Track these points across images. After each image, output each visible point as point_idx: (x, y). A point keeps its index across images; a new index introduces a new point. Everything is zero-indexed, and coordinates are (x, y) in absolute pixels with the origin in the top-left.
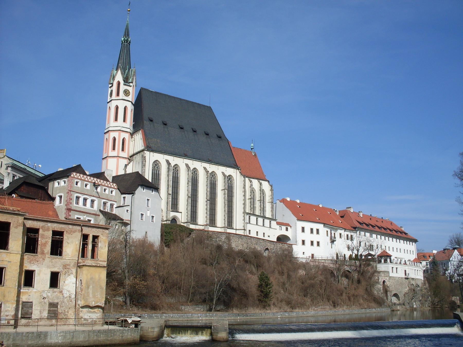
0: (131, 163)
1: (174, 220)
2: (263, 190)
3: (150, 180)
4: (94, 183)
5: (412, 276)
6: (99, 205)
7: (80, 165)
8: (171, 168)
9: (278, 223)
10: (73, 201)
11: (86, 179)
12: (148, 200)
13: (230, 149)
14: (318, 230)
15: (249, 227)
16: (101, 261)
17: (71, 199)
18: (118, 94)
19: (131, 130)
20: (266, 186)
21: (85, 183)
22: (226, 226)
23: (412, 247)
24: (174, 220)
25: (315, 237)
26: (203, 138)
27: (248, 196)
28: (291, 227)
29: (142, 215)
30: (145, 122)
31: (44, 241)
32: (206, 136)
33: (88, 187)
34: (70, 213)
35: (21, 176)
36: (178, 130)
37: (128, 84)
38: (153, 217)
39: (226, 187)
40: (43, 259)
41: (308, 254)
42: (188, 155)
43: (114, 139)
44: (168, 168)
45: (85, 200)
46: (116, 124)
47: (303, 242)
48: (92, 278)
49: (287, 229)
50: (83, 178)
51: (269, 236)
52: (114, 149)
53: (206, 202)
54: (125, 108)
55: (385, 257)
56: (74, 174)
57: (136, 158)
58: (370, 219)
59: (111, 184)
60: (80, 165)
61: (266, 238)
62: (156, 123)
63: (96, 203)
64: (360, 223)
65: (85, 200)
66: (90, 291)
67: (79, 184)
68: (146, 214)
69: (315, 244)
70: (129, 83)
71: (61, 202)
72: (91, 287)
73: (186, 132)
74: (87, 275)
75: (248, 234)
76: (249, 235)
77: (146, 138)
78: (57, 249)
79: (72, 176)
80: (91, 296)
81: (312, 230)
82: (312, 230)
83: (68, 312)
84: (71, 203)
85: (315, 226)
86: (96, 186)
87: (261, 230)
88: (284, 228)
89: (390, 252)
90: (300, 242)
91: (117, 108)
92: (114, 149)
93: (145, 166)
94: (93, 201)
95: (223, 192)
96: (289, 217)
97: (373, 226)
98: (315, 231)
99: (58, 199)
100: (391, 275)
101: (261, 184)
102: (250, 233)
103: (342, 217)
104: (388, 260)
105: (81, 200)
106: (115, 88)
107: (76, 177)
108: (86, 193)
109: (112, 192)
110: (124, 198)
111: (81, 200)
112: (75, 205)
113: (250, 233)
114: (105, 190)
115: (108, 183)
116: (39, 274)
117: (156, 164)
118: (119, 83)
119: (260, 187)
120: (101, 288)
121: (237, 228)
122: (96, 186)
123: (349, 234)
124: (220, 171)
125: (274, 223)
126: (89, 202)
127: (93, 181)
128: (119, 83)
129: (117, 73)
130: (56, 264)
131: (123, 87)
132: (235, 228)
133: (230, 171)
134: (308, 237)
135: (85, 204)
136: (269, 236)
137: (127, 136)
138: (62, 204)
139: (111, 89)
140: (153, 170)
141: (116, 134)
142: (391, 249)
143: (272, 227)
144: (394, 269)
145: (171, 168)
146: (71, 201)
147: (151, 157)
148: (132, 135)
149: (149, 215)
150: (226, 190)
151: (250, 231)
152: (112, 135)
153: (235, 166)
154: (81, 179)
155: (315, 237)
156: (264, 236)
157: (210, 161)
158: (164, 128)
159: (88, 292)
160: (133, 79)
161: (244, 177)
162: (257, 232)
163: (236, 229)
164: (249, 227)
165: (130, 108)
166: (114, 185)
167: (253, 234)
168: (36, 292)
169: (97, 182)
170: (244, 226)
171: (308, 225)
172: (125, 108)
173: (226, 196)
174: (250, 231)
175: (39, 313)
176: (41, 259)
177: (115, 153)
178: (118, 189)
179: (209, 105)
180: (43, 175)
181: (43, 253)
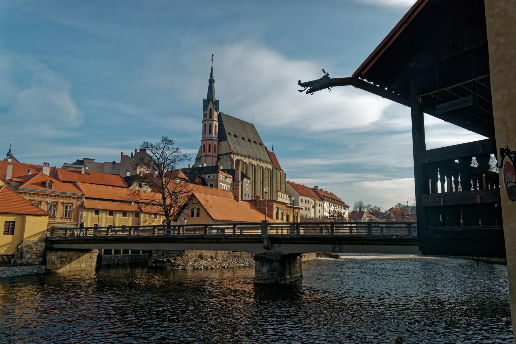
25: (308, 206)
43: (210, 145)
46: (210, 135)
52: (210, 151)
69: (307, 209)
81: (306, 201)
85: (308, 199)
92: (210, 151)
106: (208, 112)
118: (211, 110)
123: (320, 203)
125: (287, 196)
128: (211, 110)
129: (209, 103)
137: (216, 143)
139: (206, 112)
141: (211, 142)
147: (236, 158)
148: (218, 143)
152: (209, 142)
155: (308, 206)
171: (304, 198)
172: (216, 126)
177: (211, 154)
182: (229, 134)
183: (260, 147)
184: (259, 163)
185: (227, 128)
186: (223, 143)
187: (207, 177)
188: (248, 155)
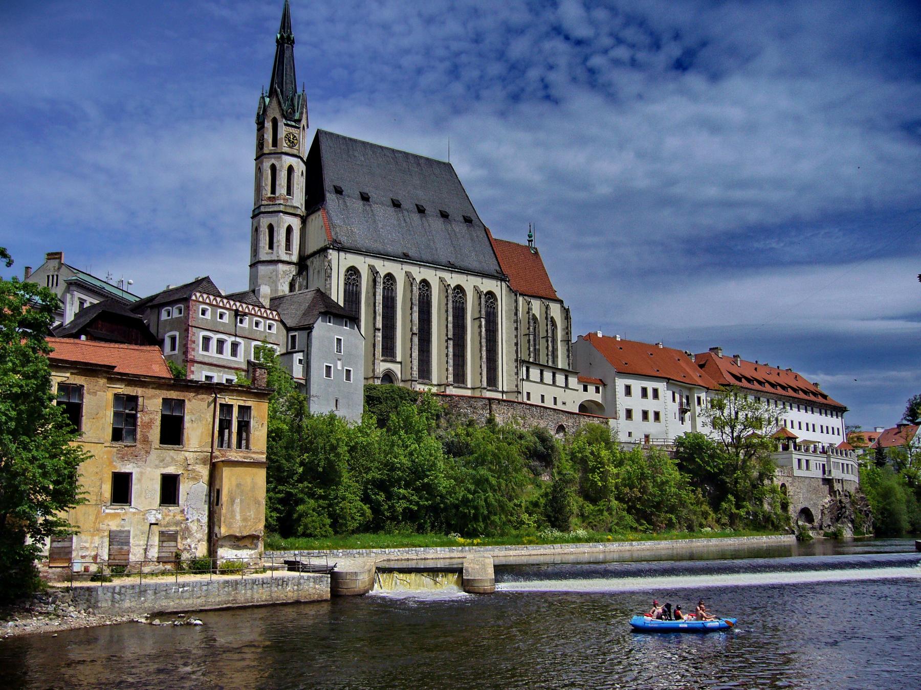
0: (304, 273)
1: (388, 377)
2: (552, 318)
3: (341, 303)
4: (237, 311)
5: (836, 474)
6: (247, 351)
7: (208, 277)
8: (380, 280)
9: (580, 381)
10: (198, 345)
11: (221, 304)
12: (339, 340)
13: (488, 243)
14: (655, 391)
15: (527, 387)
16: (254, 453)
17: (194, 342)
18: (275, 143)
19: (302, 211)
20: (555, 311)
21: (220, 310)
22: (485, 384)
23: (835, 422)
24: (388, 377)
25: (651, 405)
26: (437, 224)
27: (523, 329)
28: (604, 385)
29: (328, 368)
30: (328, 195)
31: (146, 419)
32: (442, 219)
33: (226, 319)
34: (193, 369)
35: (96, 302)
36: (391, 210)
37: (293, 124)
38: (348, 371)
39: (483, 312)
40: (148, 452)
41: (638, 436)
42: (410, 254)
44: (375, 281)
45: (221, 343)
47: (629, 414)
48: (238, 485)
49: (597, 391)
50: (214, 303)
51: (564, 403)
53: (447, 341)
54: (290, 169)
55: (787, 441)
56: (198, 294)
57: (312, 262)
58: (756, 369)
59: (269, 312)
60: (208, 277)
61: (559, 406)
62: (349, 196)
63: (241, 350)
64: (738, 379)
65: (221, 343)
66: (237, 508)
67: (208, 316)
68: (336, 366)
69: (651, 416)
70: (295, 121)
71: (173, 348)
72: (238, 501)
73: (406, 213)
74: (230, 479)
75: (525, 400)
76: (528, 402)
77: (329, 225)
78: (172, 432)
79: (194, 298)
80: (238, 517)
81: (644, 390)
82: (644, 390)
83: (196, 548)
84: (193, 350)
85: (650, 385)
86: (238, 315)
87: (550, 393)
88: (591, 389)
89: (795, 432)
90: (622, 414)
91: (273, 168)
92: (271, 246)
93: (330, 277)
94: (235, 346)
95: (477, 323)
96: (604, 368)
97: (760, 383)
98: (650, 393)
99: (168, 342)
100: (797, 473)
101: (547, 307)
102: (529, 399)
103: (702, 366)
104: (792, 446)
105: (213, 345)
107: (201, 299)
108: (222, 329)
109: (270, 327)
110: (294, 337)
111: (213, 345)
112: (201, 352)
113: (529, 399)
114: (257, 324)
115: (263, 310)
116: (139, 480)
117: (353, 272)
118: (275, 122)
119: (546, 313)
120: (257, 502)
121: (505, 390)
122: (238, 315)
124: (469, 283)
126: (227, 347)
127: (234, 308)
128: (275, 122)
130: (171, 461)
131: (283, 131)
132: (500, 389)
133: (488, 285)
134: (637, 403)
135: (220, 350)
136: (564, 403)
137: (296, 223)
138: (176, 352)
140: (345, 284)
142: (796, 425)
143: (570, 386)
144: (804, 463)
145: (380, 280)
146: (193, 346)
148: (304, 220)
149: (339, 368)
150: (483, 320)
151: (528, 394)
153: (500, 276)
154: (210, 304)
155: (651, 405)
156: (555, 403)
157: (452, 267)
158: (364, 205)
159: (233, 512)
160: (302, 113)
161: (516, 295)
162: (543, 396)
163: (503, 392)
164: (527, 387)
165: (300, 168)
166: (275, 313)
167: (535, 400)
168: (134, 514)
169: (240, 309)
170: (517, 386)
171: (637, 385)
172: (290, 169)
173: (483, 330)
174: (528, 394)
175: (142, 552)
176: (143, 452)
178: (282, 322)
179: (447, 161)
180: (138, 299)
181: (146, 441)
182: (338, 191)
183: (460, 228)
184: (446, 276)
185: (330, 177)
186: (317, 220)
187: (164, 316)
188: (399, 250)
